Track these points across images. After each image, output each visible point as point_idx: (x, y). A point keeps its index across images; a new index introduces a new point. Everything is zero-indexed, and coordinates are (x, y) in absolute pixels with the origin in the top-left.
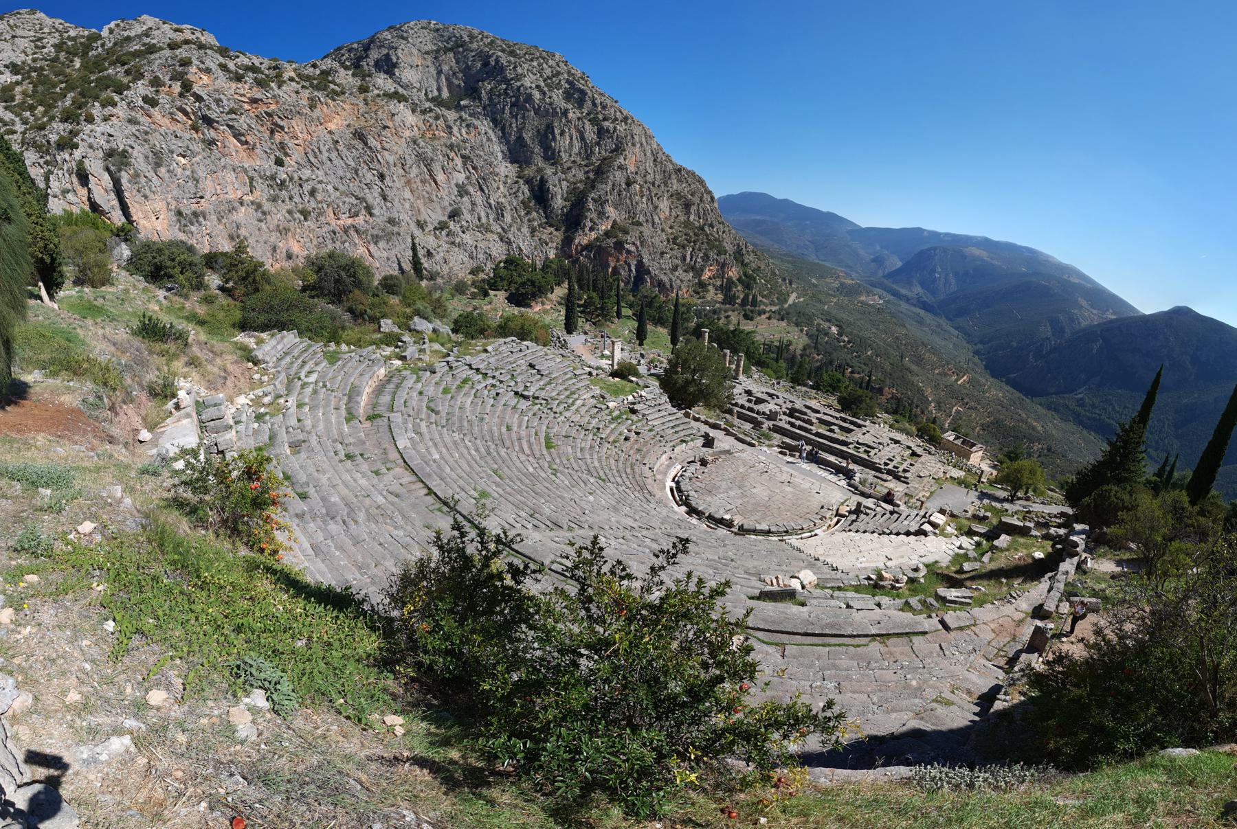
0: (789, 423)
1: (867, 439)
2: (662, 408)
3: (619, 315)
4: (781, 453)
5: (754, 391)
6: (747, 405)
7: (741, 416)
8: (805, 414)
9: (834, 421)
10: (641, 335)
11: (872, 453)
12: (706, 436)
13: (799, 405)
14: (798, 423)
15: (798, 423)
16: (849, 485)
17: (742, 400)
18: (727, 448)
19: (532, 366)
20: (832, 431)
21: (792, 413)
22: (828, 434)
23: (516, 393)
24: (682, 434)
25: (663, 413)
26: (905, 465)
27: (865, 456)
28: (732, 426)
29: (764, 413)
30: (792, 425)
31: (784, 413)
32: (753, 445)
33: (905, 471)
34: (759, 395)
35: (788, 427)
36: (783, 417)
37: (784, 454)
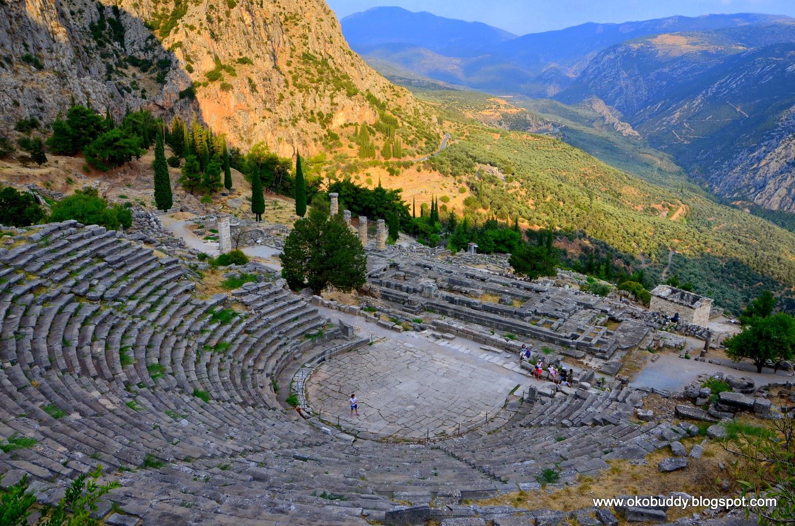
1: (548, 307)
2: (280, 296)
3: (228, 184)
4: (434, 335)
5: (402, 264)
6: (394, 282)
7: (385, 297)
8: (467, 285)
10: (258, 208)
11: (556, 324)
14: (458, 297)
15: (458, 297)
16: (522, 367)
17: (387, 278)
18: (365, 338)
19: (101, 258)
23: (79, 296)
26: (598, 338)
27: (545, 329)
28: (371, 309)
29: (415, 291)
31: (441, 288)
33: (599, 342)
34: (408, 268)
35: (445, 303)
37: (438, 338)
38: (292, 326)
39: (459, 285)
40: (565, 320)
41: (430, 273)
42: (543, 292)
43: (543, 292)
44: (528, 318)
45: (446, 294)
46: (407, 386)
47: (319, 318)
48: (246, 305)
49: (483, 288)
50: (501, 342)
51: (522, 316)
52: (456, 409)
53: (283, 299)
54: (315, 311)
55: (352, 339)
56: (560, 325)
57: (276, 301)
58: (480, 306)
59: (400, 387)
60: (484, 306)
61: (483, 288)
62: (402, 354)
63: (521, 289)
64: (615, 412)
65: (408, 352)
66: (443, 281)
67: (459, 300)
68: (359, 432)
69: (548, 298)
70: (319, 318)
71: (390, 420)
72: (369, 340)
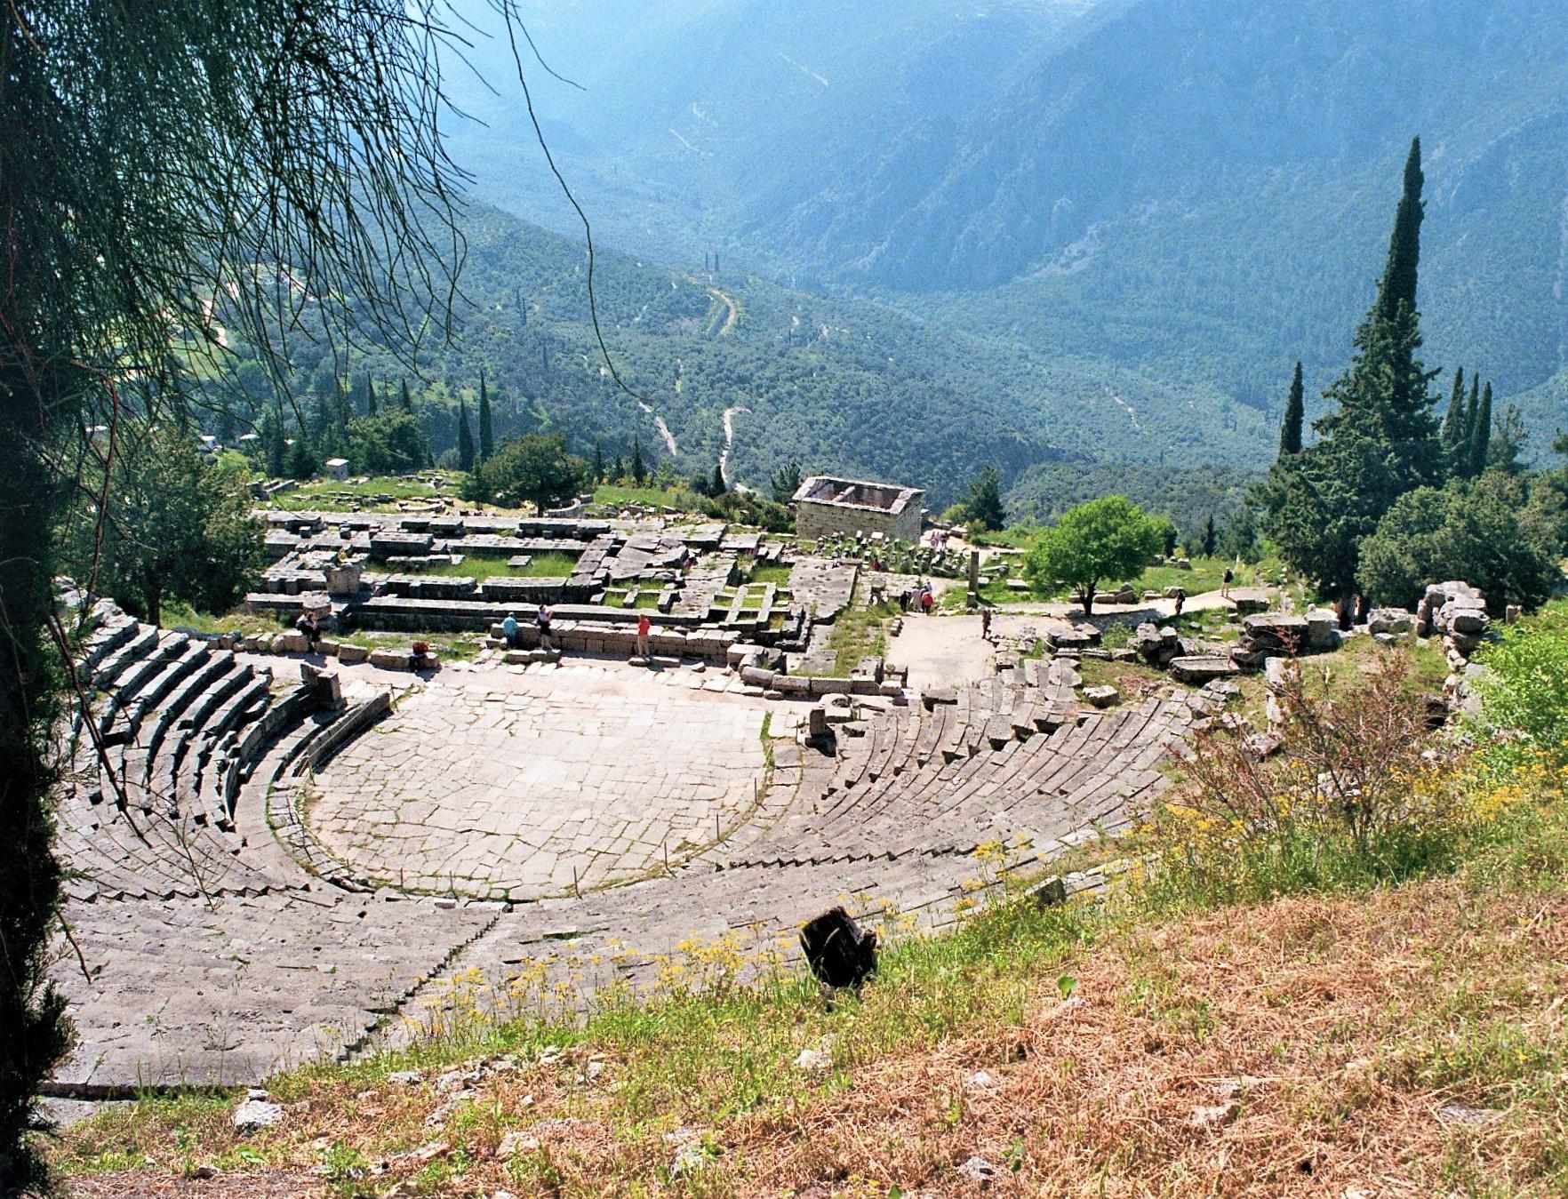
4: (511, 661)
13: (389, 525)
15: (416, 581)
16: (748, 681)
21: (380, 554)
24: (237, 698)
29: (302, 585)
30: (403, 591)
35: (391, 600)
38: (202, 700)
40: (681, 585)
41: (316, 539)
42: (607, 531)
43: (607, 531)
44: (597, 598)
46: (543, 774)
47: (248, 675)
49: (457, 550)
50: (671, 640)
51: (582, 595)
52: (676, 793)
53: (152, 644)
54: (228, 665)
56: (675, 598)
57: (137, 654)
58: (479, 590)
59: (528, 778)
61: (457, 550)
62: (479, 711)
64: (1049, 705)
68: (507, 890)
69: (622, 543)
70: (248, 675)
71: (556, 848)
72: (387, 695)
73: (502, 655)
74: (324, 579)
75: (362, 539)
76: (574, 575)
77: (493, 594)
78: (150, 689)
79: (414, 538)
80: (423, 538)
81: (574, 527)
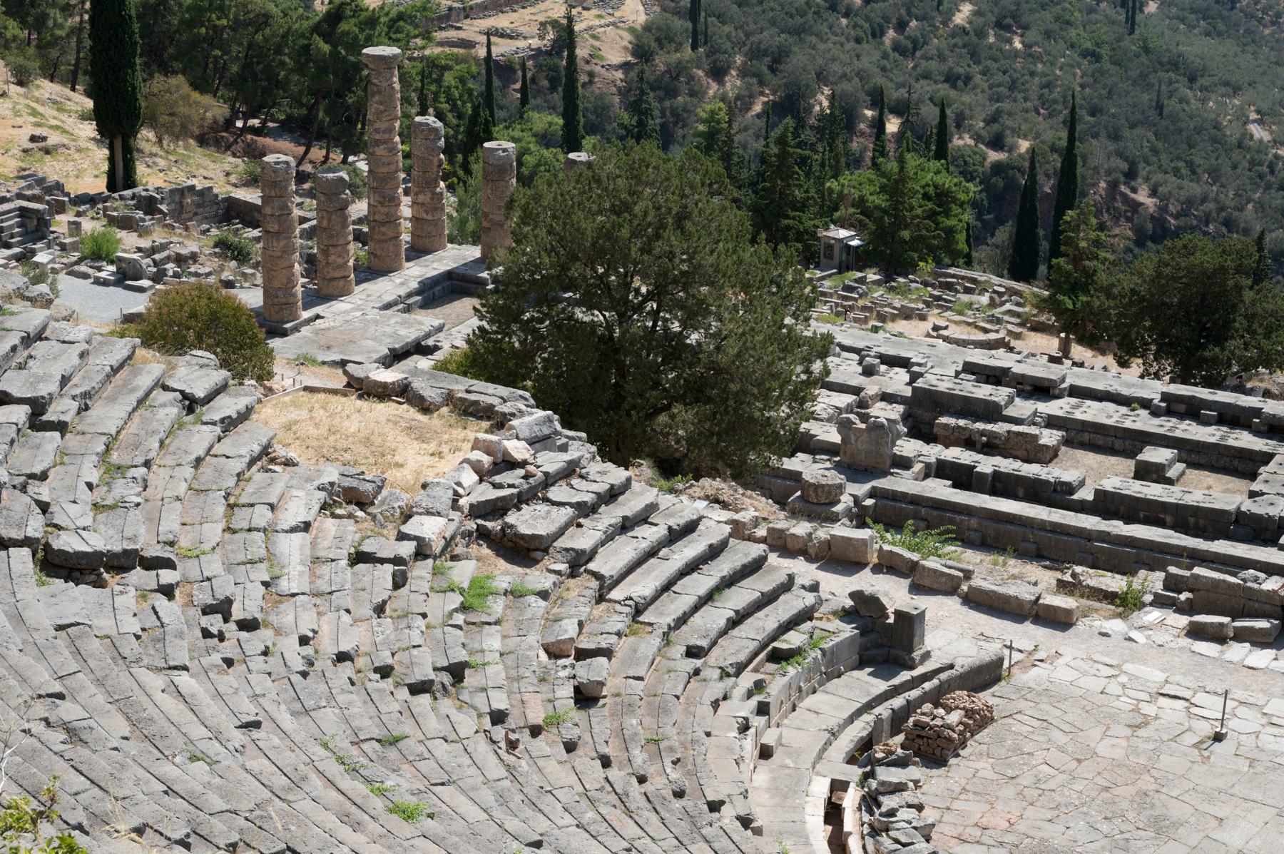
0: (941, 470)
4: (1196, 632)
8: (991, 412)
9: (1142, 421)
12: (864, 610)
14: (986, 464)
15: (986, 464)
20: (1147, 472)
21: (924, 413)
22: (1153, 491)
24: (768, 620)
25: (649, 535)
30: (963, 477)
32: (1059, 621)
35: (940, 489)
36: (908, 447)
37: (1218, 636)
39: (960, 414)
45: (934, 452)
48: (523, 551)
49: (1052, 422)
55: (927, 656)
57: (626, 526)
58: (1086, 494)
60: (1101, 494)
62: (1148, 709)
63: (1206, 422)
65: (1163, 701)
66: (887, 398)
67: (997, 475)
73: (1184, 620)
74: (836, 438)
75: (897, 381)
76: (1253, 495)
77: (1107, 504)
78: (642, 585)
79: (984, 391)
80: (1001, 394)
81: (1257, 412)
